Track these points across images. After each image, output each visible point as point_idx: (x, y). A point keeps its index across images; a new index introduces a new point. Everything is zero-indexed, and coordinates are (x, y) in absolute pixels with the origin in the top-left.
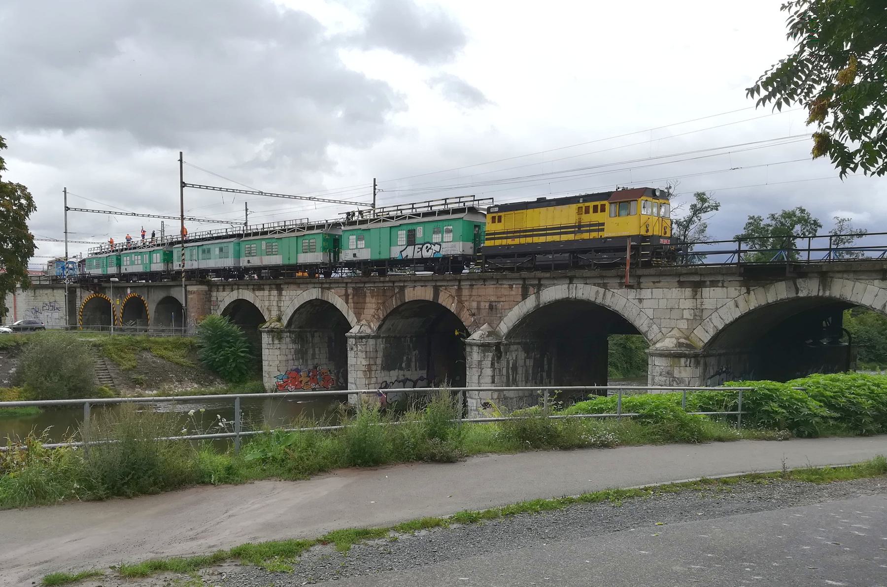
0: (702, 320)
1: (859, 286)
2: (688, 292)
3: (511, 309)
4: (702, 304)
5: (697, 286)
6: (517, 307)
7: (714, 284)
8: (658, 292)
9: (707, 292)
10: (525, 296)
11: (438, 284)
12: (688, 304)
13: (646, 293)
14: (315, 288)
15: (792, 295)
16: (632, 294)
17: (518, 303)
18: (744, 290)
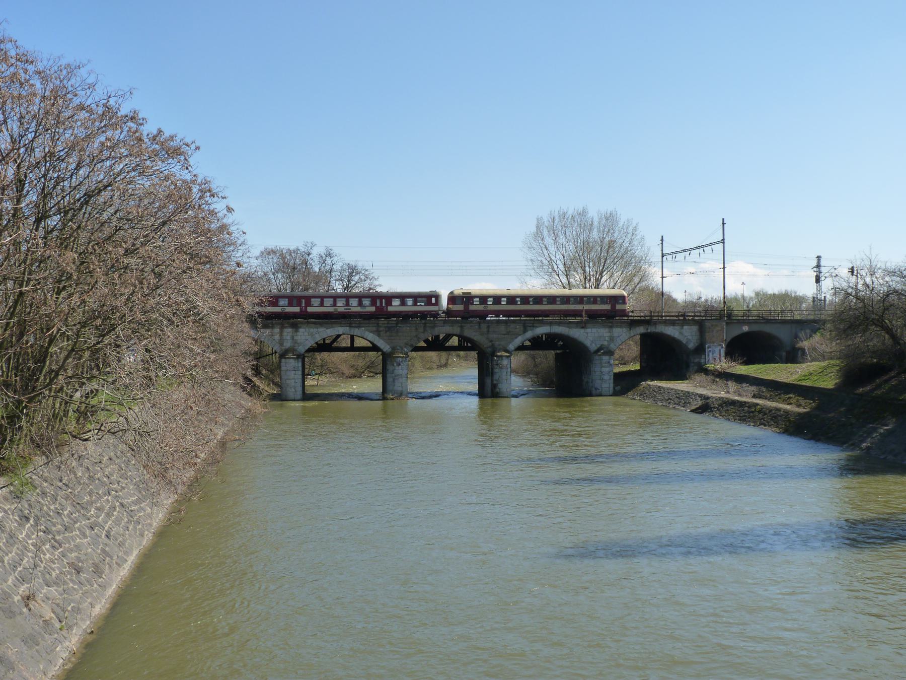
0: (613, 340)
1: (667, 328)
2: (607, 330)
3: (516, 338)
4: (613, 334)
5: (611, 327)
6: (520, 337)
7: (617, 327)
8: (594, 330)
9: (614, 330)
10: (525, 331)
11: (463, 325)
12: (608, 334)
13: (589, 330)
14: (341, 326)
15: (646, 331)
16: (582, 331)
17: (520, 335)
18: (628, 329)
